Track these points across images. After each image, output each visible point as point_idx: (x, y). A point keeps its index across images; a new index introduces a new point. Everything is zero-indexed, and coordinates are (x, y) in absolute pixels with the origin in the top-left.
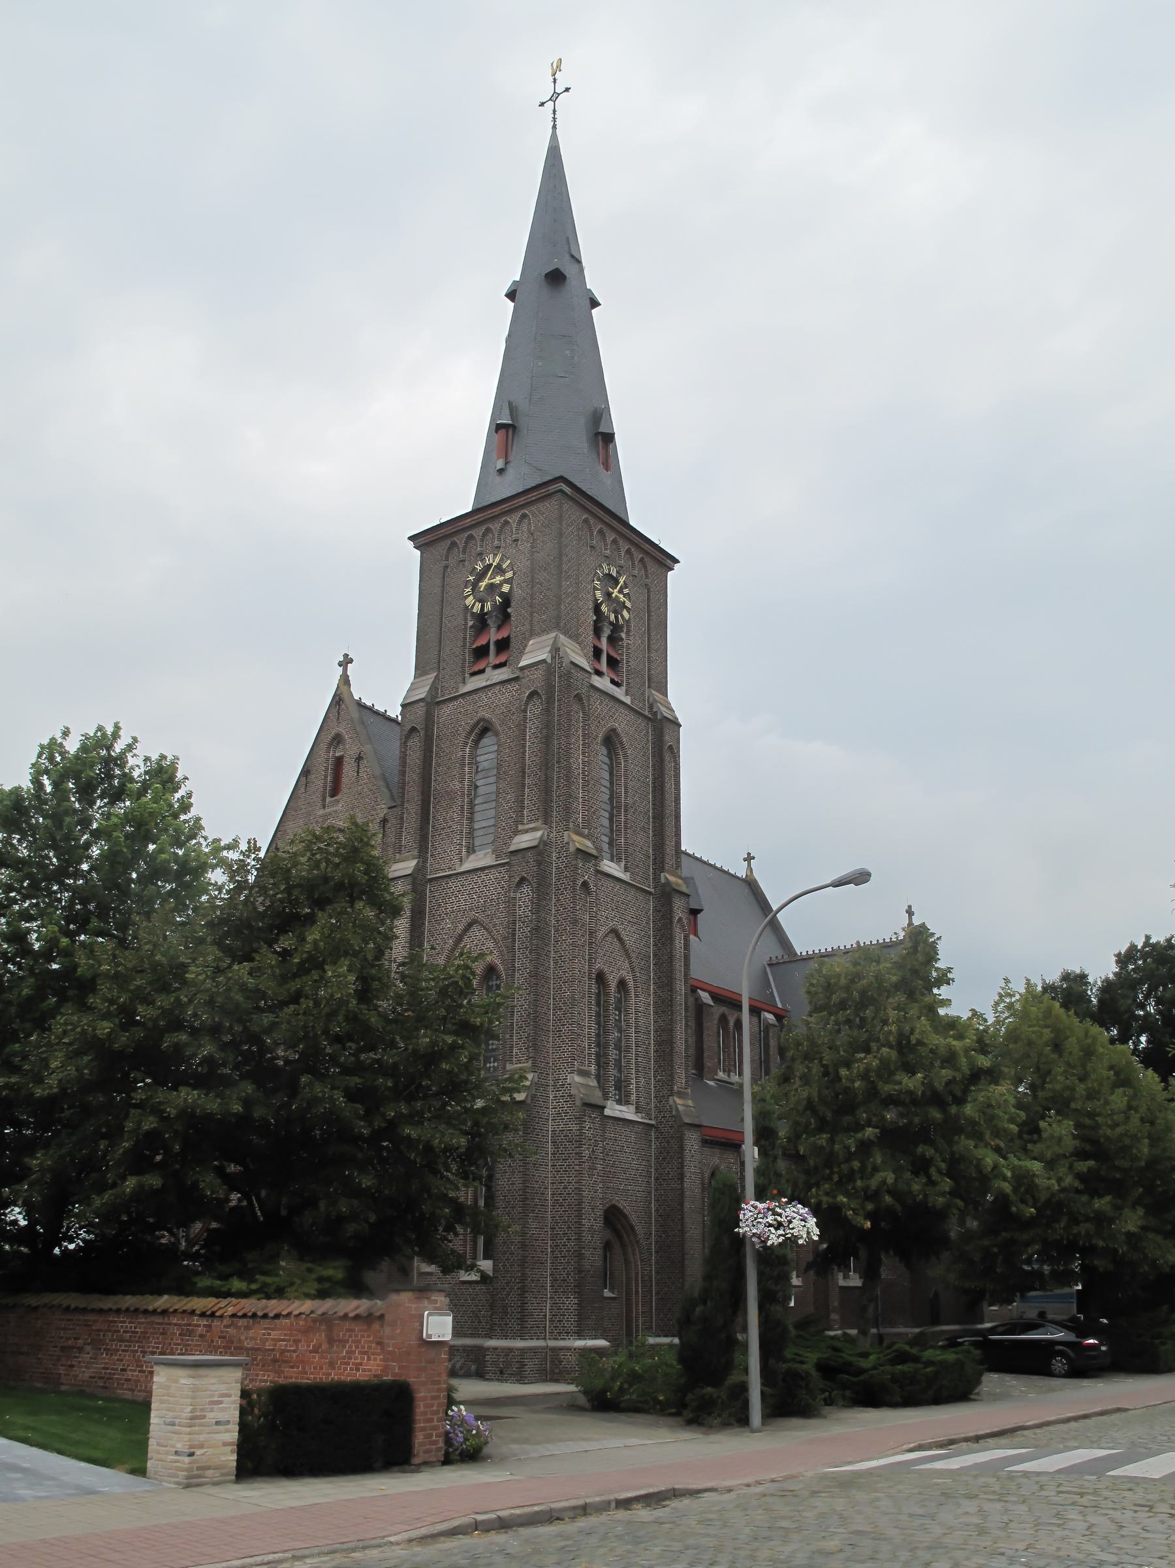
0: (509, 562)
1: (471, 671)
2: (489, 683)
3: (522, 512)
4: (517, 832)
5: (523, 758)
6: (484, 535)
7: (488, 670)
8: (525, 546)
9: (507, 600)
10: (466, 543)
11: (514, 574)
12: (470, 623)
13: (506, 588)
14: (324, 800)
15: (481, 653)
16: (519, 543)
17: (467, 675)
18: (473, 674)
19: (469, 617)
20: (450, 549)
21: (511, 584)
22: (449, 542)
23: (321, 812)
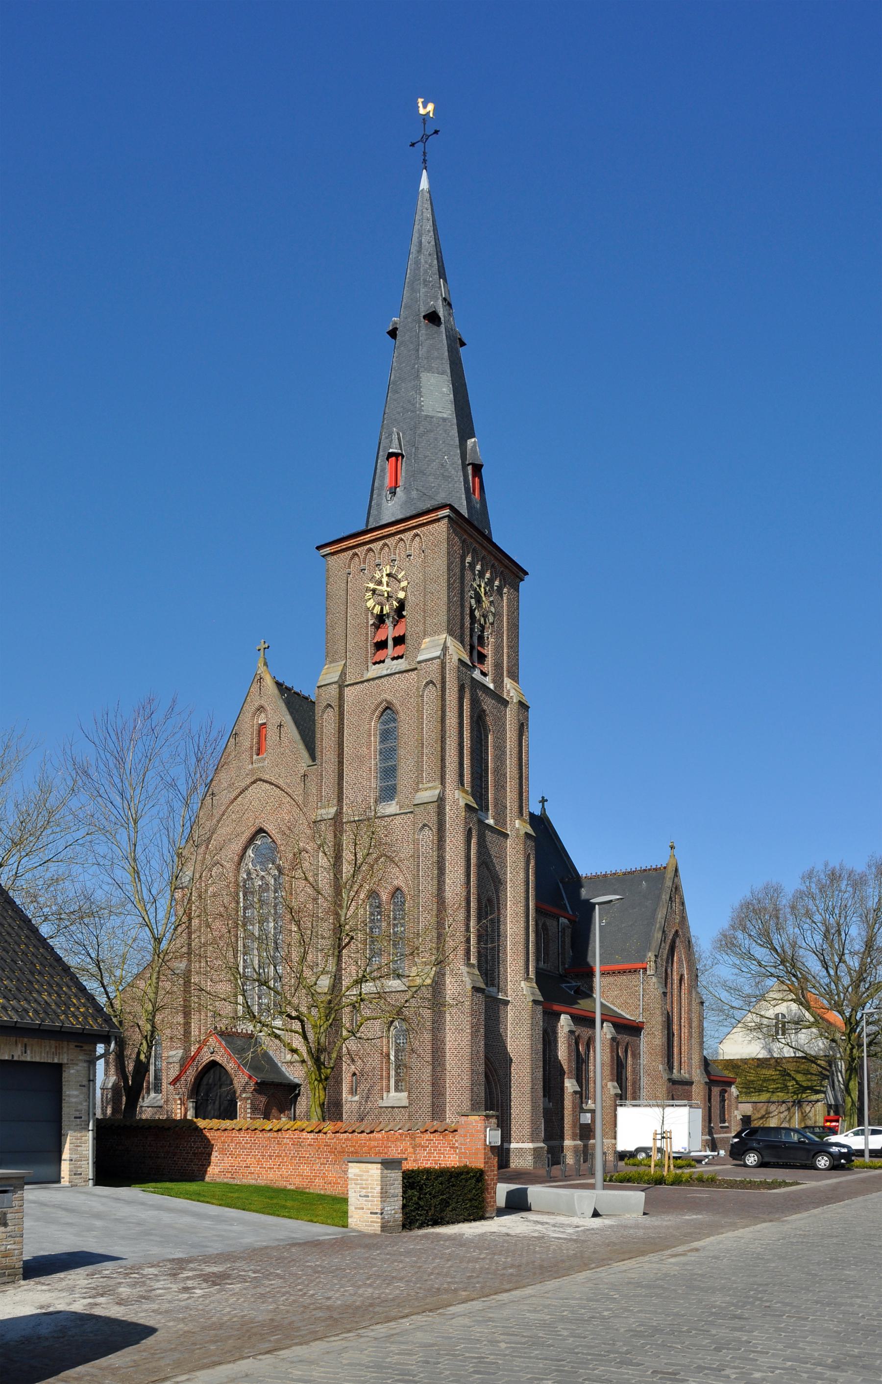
0: (403, 573)
1: (374, 661)
2: (389, 672)
3: (414, 531)
4: (417, 790)
5: (422, 732)
6: (382, 549)
7: (388, 661)
8: (416, 560)
9: (402, 605)
10: (366, 554)
11: (408, 583)
12: (371, 622)
13: (401, 595)
14: (252, 757)
15: (381, 645)
16: (412, 557)
17: (370, 664)
18: (374, 664)
19: (370, 617)
20: (352, 558)
21: (406, 591)
22: (351, 552)
23: (250, 767)
